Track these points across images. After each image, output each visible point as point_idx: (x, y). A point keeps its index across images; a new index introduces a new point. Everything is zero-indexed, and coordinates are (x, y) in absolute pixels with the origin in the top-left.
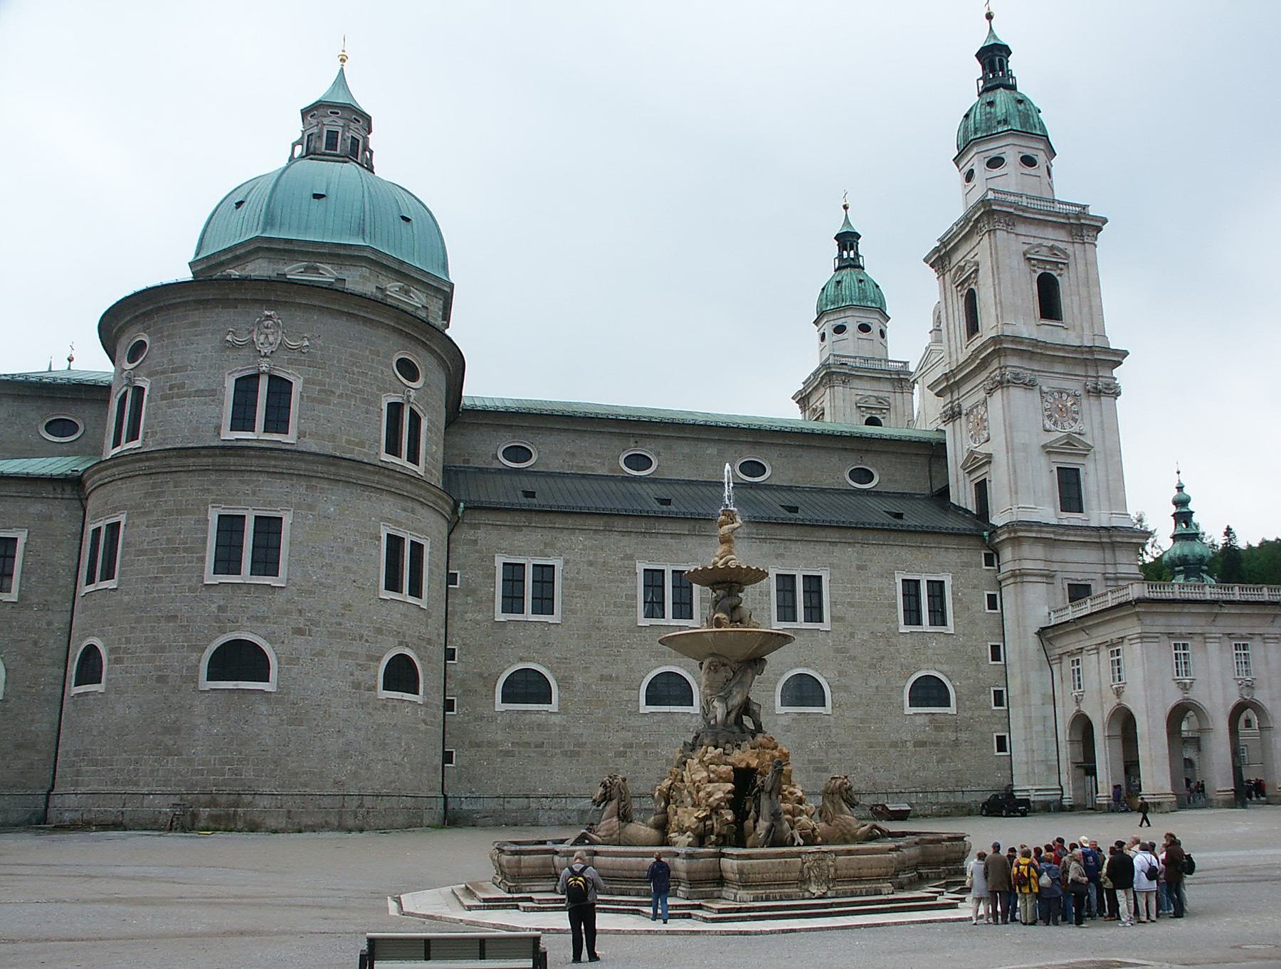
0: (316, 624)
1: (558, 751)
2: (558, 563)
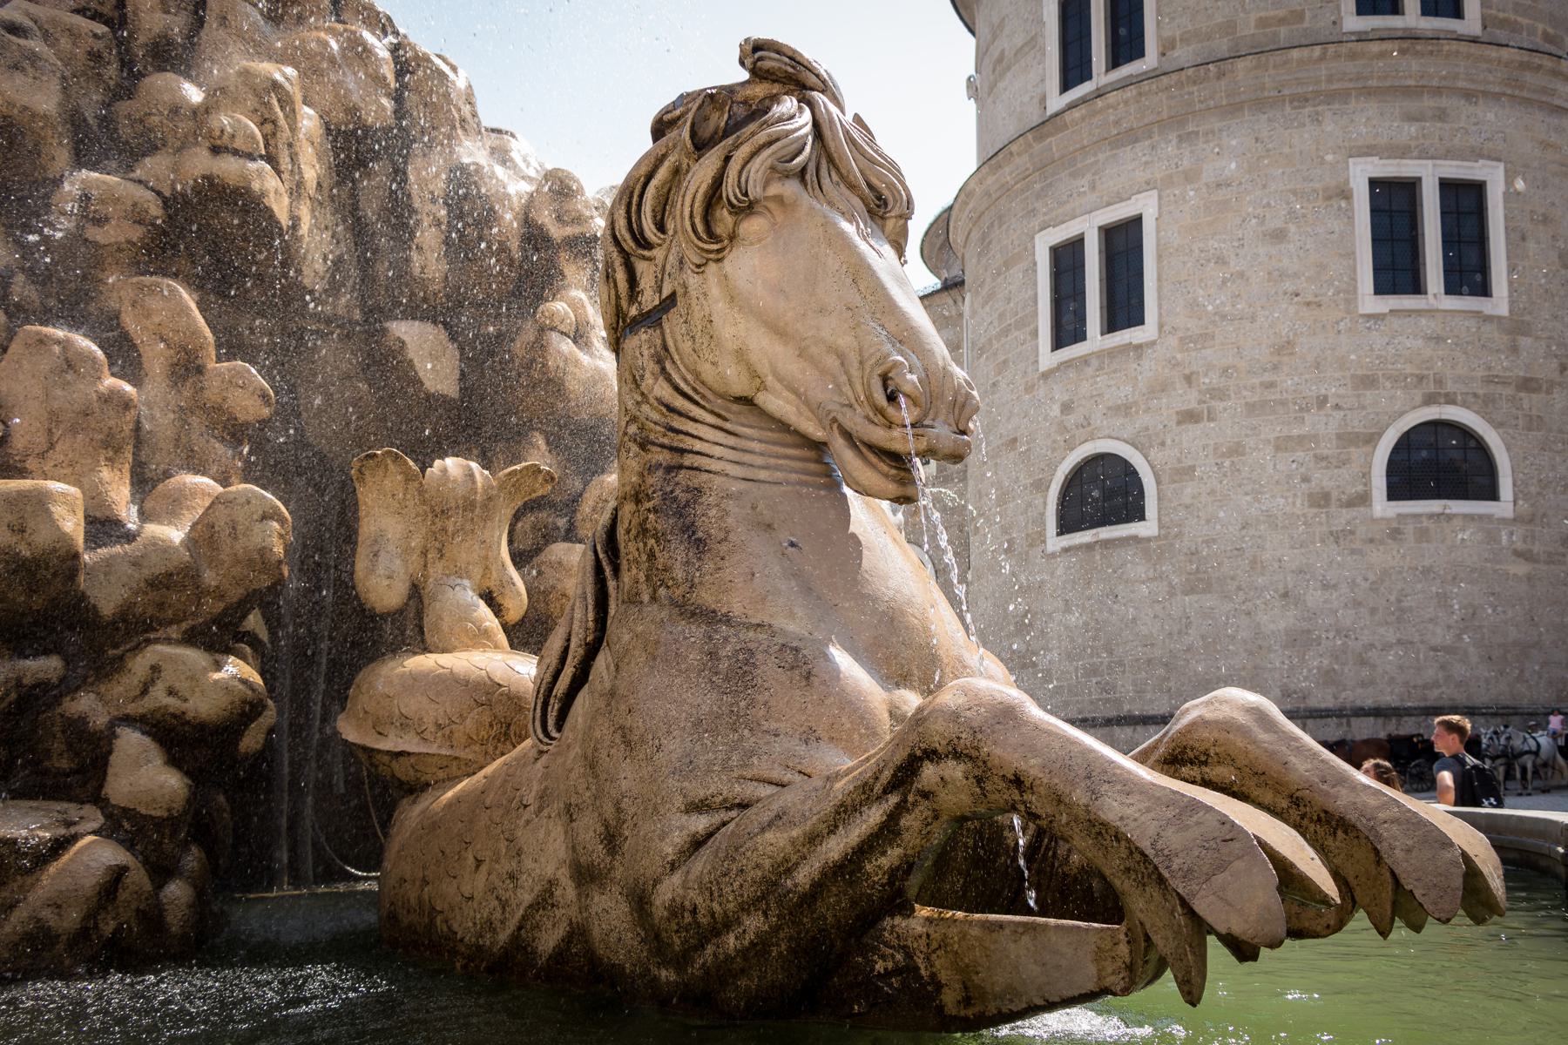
0: (1219, 393)
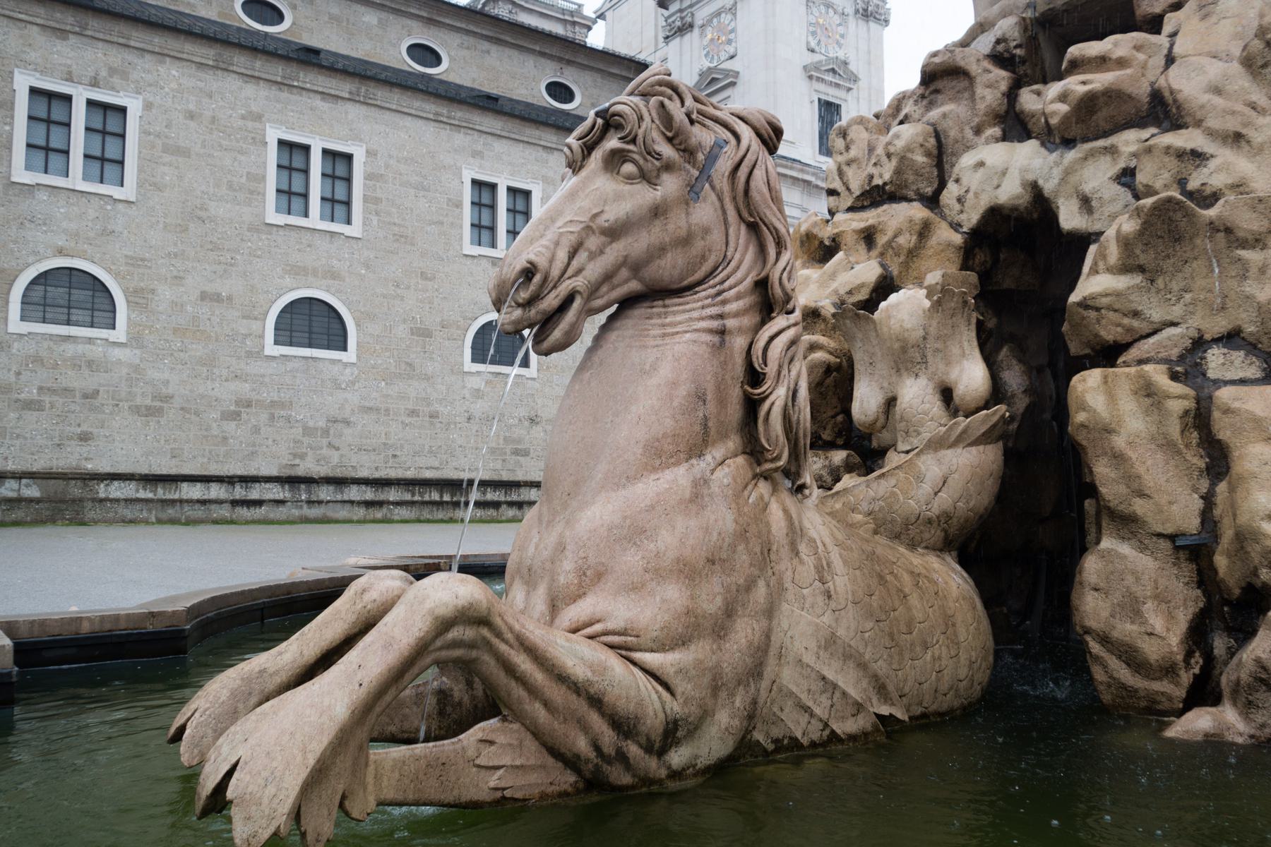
1: (126, 405)
2: (134, 107)
